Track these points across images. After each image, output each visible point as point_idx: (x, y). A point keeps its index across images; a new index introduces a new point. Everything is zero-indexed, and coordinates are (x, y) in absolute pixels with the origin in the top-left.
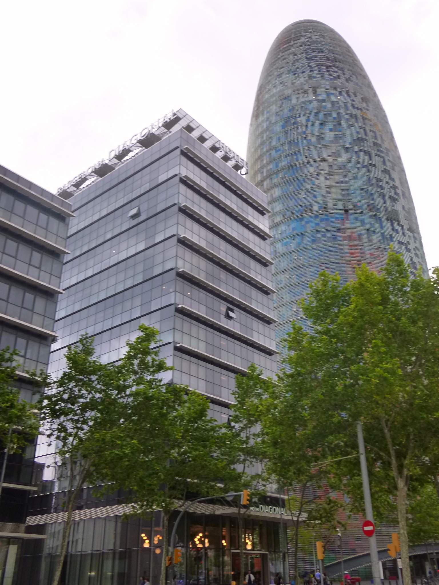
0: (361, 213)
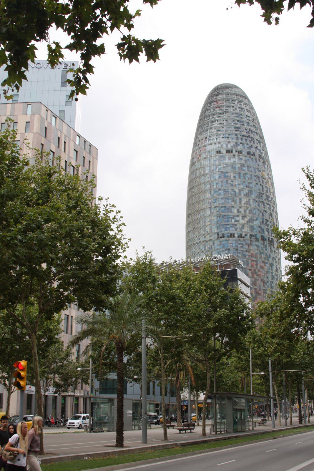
0: (258, 241)
